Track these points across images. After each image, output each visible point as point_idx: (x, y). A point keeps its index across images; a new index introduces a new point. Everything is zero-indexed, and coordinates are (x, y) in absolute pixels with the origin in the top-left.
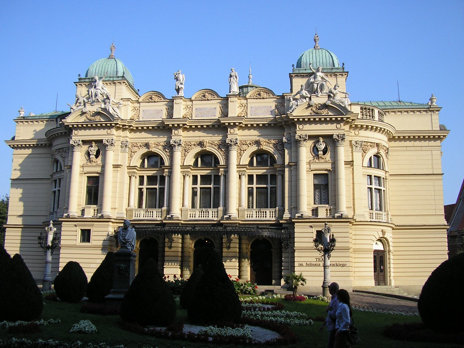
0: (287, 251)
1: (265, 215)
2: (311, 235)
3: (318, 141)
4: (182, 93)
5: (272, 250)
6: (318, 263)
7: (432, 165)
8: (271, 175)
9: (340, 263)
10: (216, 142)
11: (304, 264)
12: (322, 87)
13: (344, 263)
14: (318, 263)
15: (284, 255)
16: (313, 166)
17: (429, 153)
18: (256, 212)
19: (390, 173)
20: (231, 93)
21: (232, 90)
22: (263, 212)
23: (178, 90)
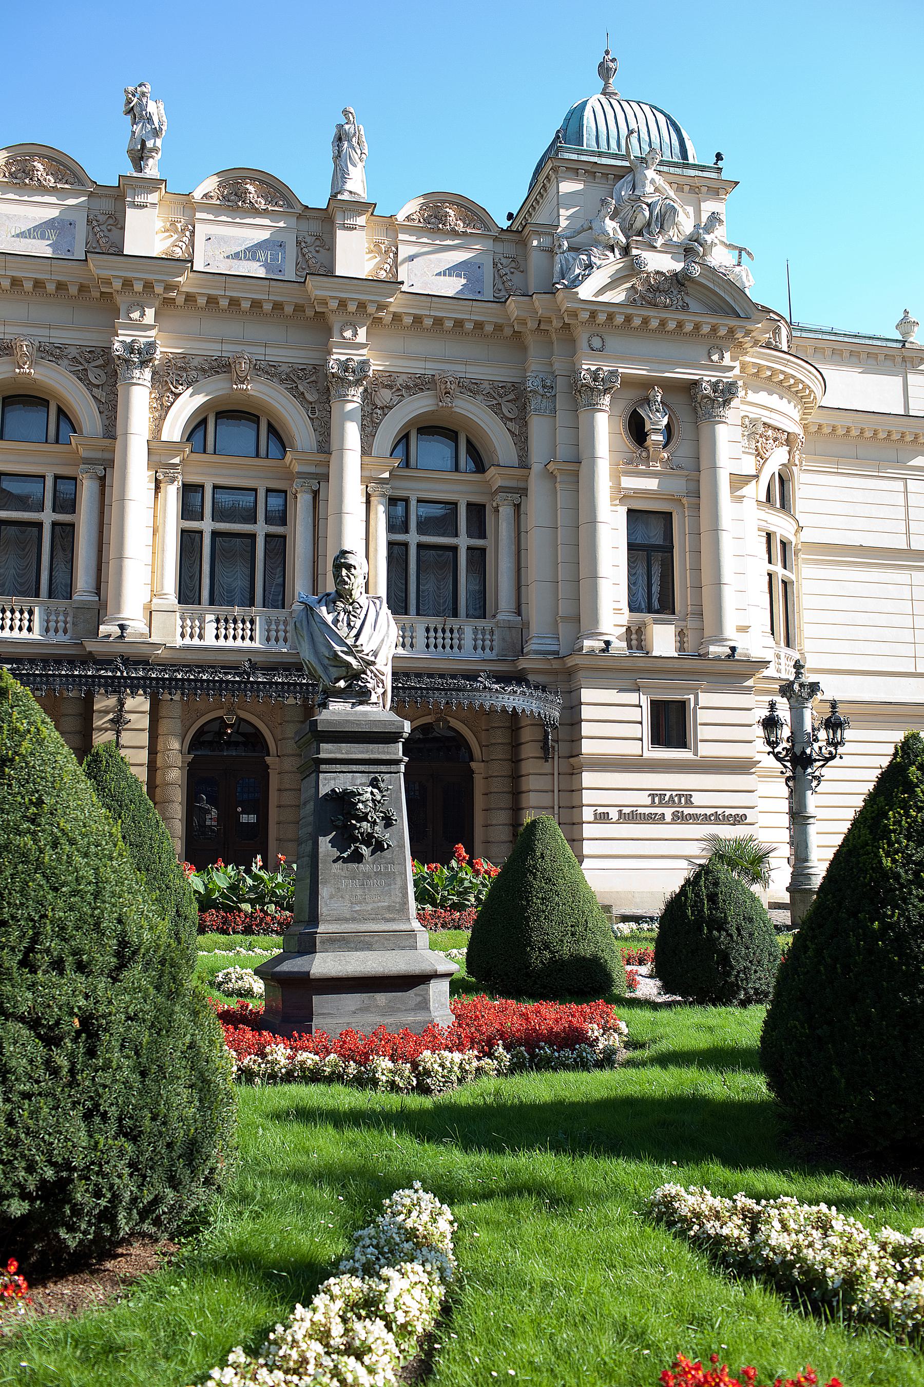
0: (547, 767)
1: (456, 642)
2: (634, 714)
3: (647, 401)
4: (152, 170)
5: (473, 765)
6: (659, 811)
7: (907, 520)
8: (469, 505)
9: (728, 812)
10: (284, 368)
11: (614, 814)
12: (664, 218)
13: (741, 812)
14: (659, 811)
15: (531, 783)
16: (630, 483)
17: (899, 485)
18: (428, 630)
19: (805, 536)
20: (345, 196)
21: (349, 186)
22: (452, 631)
23: (139, 156)
